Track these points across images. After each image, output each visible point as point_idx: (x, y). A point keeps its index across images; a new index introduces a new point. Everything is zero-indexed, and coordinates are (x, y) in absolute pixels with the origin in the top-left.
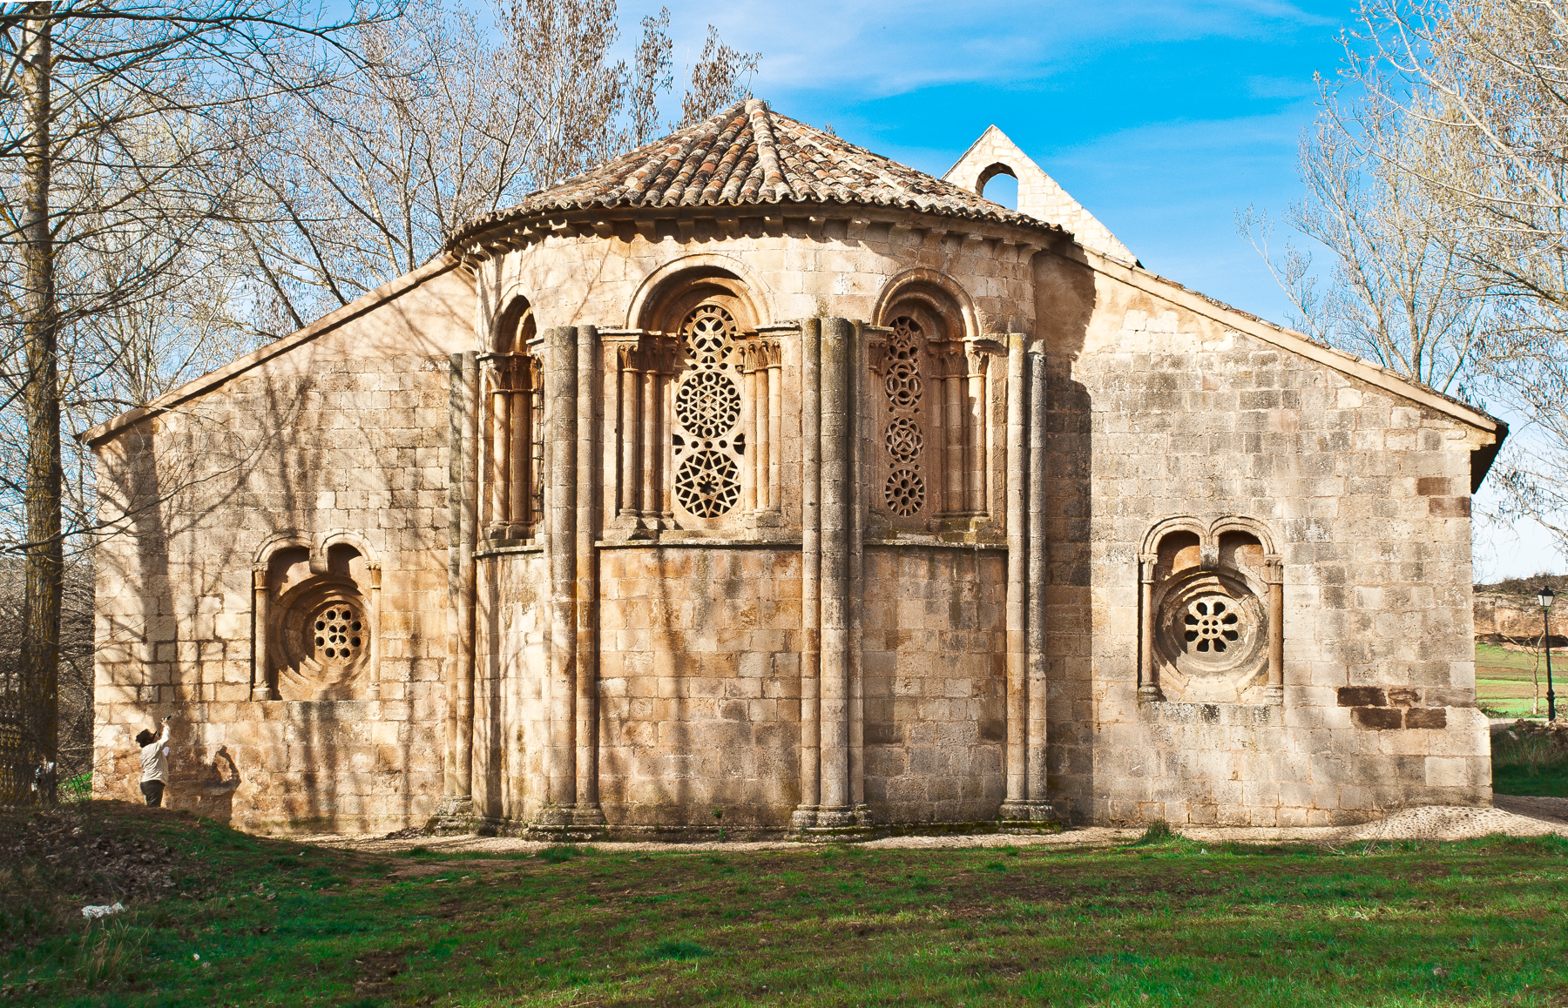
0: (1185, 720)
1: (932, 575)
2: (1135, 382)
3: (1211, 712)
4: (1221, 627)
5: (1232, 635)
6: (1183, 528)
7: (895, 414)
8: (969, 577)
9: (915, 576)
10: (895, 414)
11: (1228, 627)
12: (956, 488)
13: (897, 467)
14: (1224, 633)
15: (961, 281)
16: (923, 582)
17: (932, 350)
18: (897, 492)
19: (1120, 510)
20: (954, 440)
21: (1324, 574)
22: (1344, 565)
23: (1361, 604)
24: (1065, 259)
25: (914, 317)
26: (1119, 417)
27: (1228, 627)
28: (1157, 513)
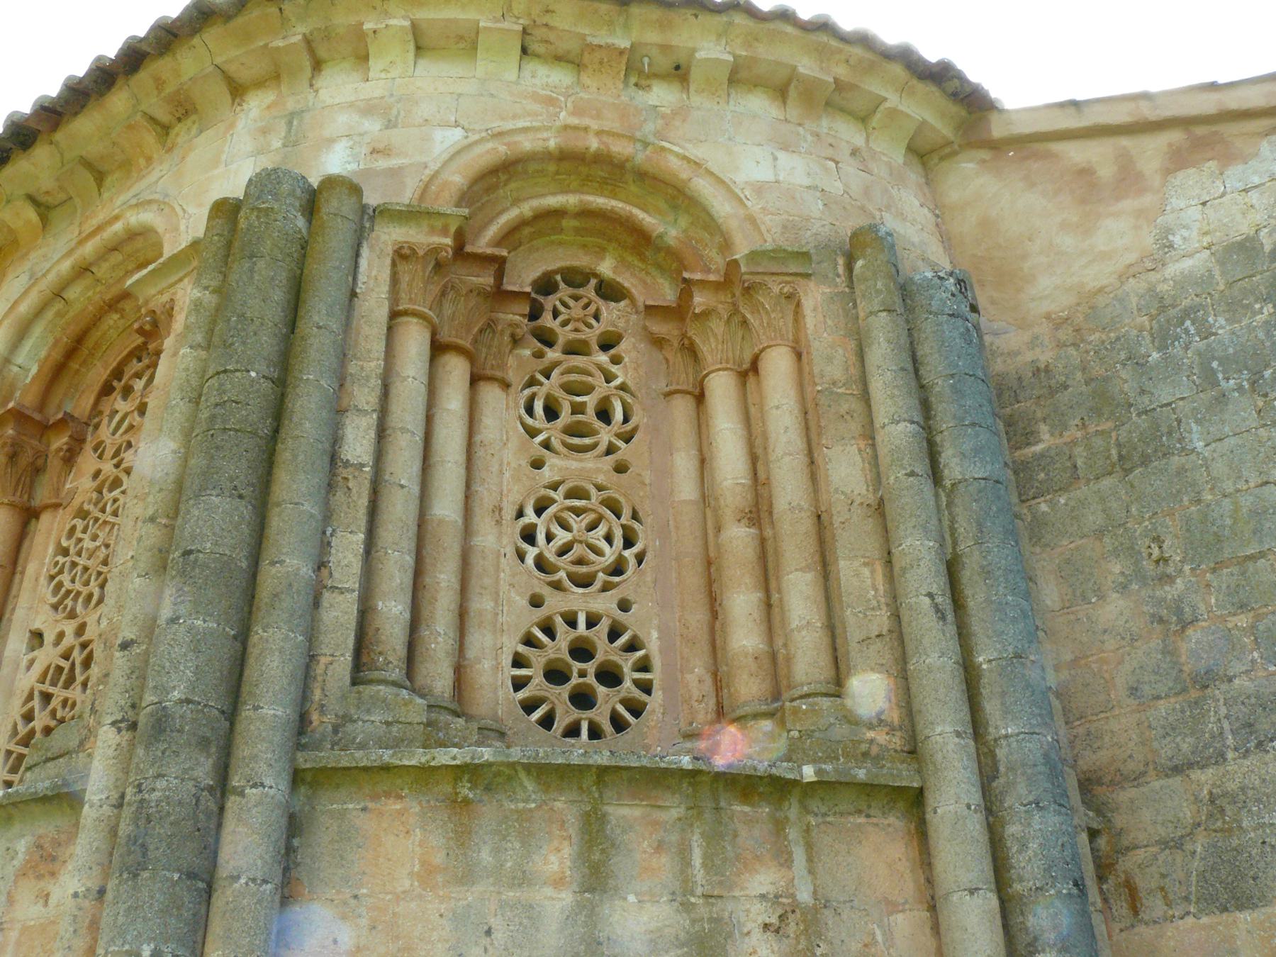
1: (596, 878)
2: (1234, 308)
7: (547, 474)
8: (763, 880)
9: (523, 879)
10: (547, 474)
12: (745, 637)
13: (555, 604)
15: (695, 152)
16: (556, 903)
17: (660, 328)
18: (556, 675)
20: (728, 515)
24: (996, 146)
25: (606, 268)
26: (1222, 398)
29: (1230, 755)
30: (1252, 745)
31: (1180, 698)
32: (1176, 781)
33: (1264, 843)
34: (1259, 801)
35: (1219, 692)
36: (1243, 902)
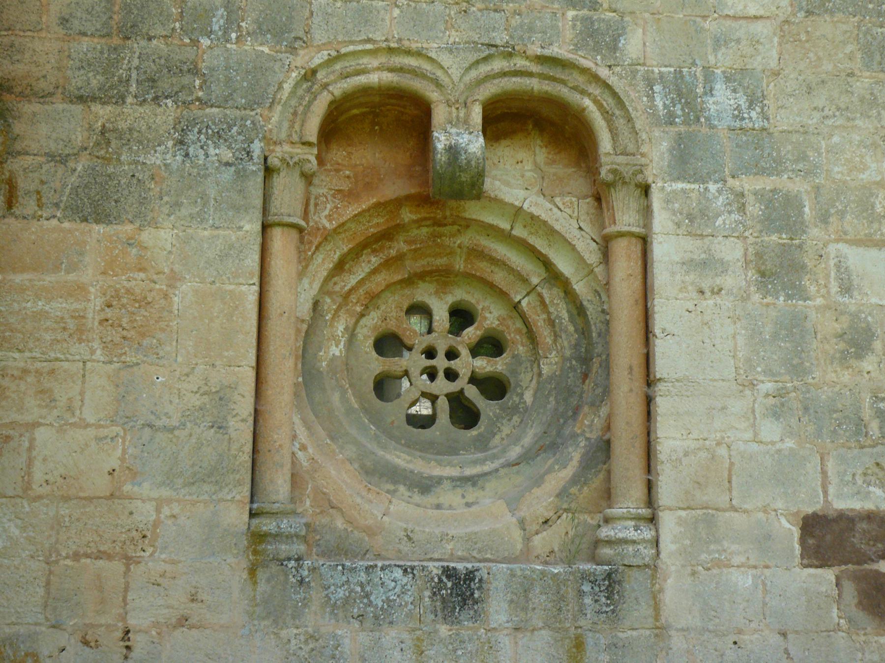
0: (381, 618)
3: (459, 591)
4: (466, 364)
5: (494, 387)
6: (387, 77)
11: (483, 365)
14: (474, 380)
19: (217, 23)
21: (754, 209)
22: (799, 186)
23: (847, 289)
27: (483, 365)
28: (319, 36)
29: (129, 100)
30: (149, 97)
31: (103, 41)
32: (78, 109)
33: (133, 176)
34: (140, 142)
35: (138, 45)
36: (101, 217)
